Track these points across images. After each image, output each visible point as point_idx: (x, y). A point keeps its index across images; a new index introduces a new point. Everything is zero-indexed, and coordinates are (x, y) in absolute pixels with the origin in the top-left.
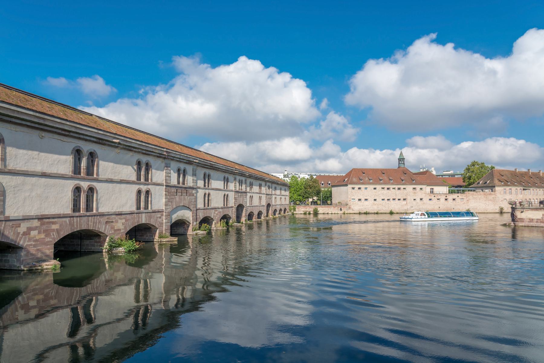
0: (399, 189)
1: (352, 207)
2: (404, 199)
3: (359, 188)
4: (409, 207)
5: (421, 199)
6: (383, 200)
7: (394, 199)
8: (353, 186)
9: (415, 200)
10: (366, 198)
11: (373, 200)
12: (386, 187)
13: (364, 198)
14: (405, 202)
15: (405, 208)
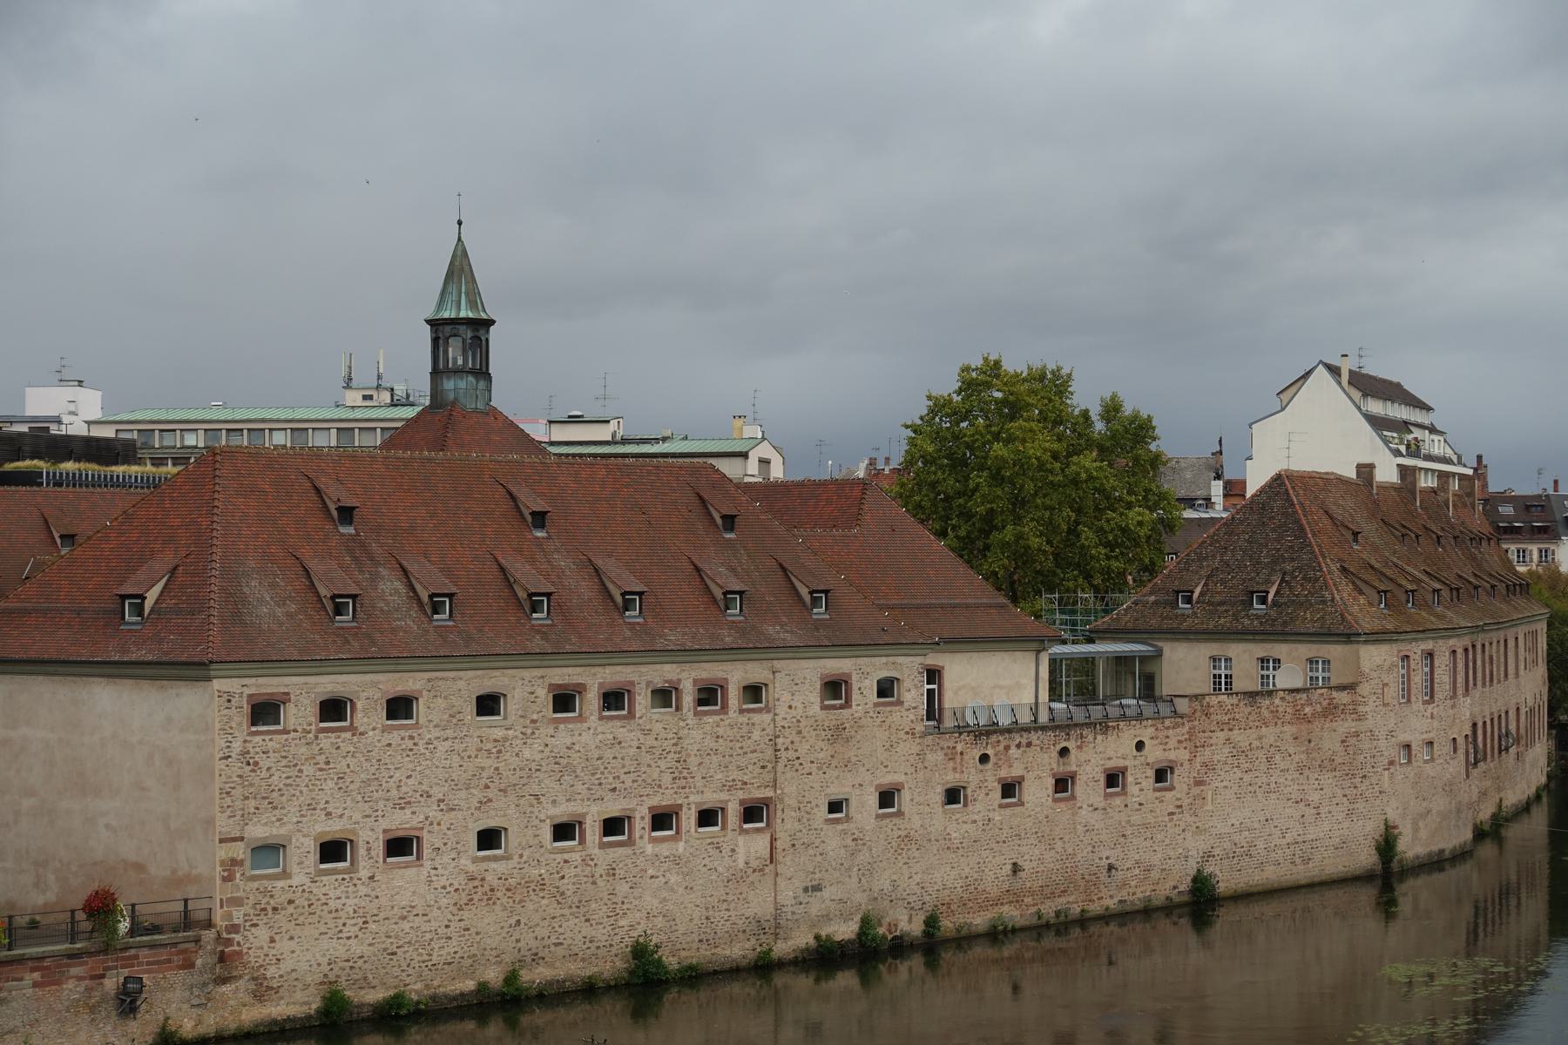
0: (709, 695)
1: (255, 942)
2: (752, 813)
3: (333, 709)
4: (787, 895)
5: (887, 798)
6: (563, 831)
7: (662, 820)
8: (269, 685)
9: (835, 807)
10: (400, 822)
11: (473, 841)
12: (594, 679)
13: (384, 824)
14: (751, 845)
15: (759, 903)
